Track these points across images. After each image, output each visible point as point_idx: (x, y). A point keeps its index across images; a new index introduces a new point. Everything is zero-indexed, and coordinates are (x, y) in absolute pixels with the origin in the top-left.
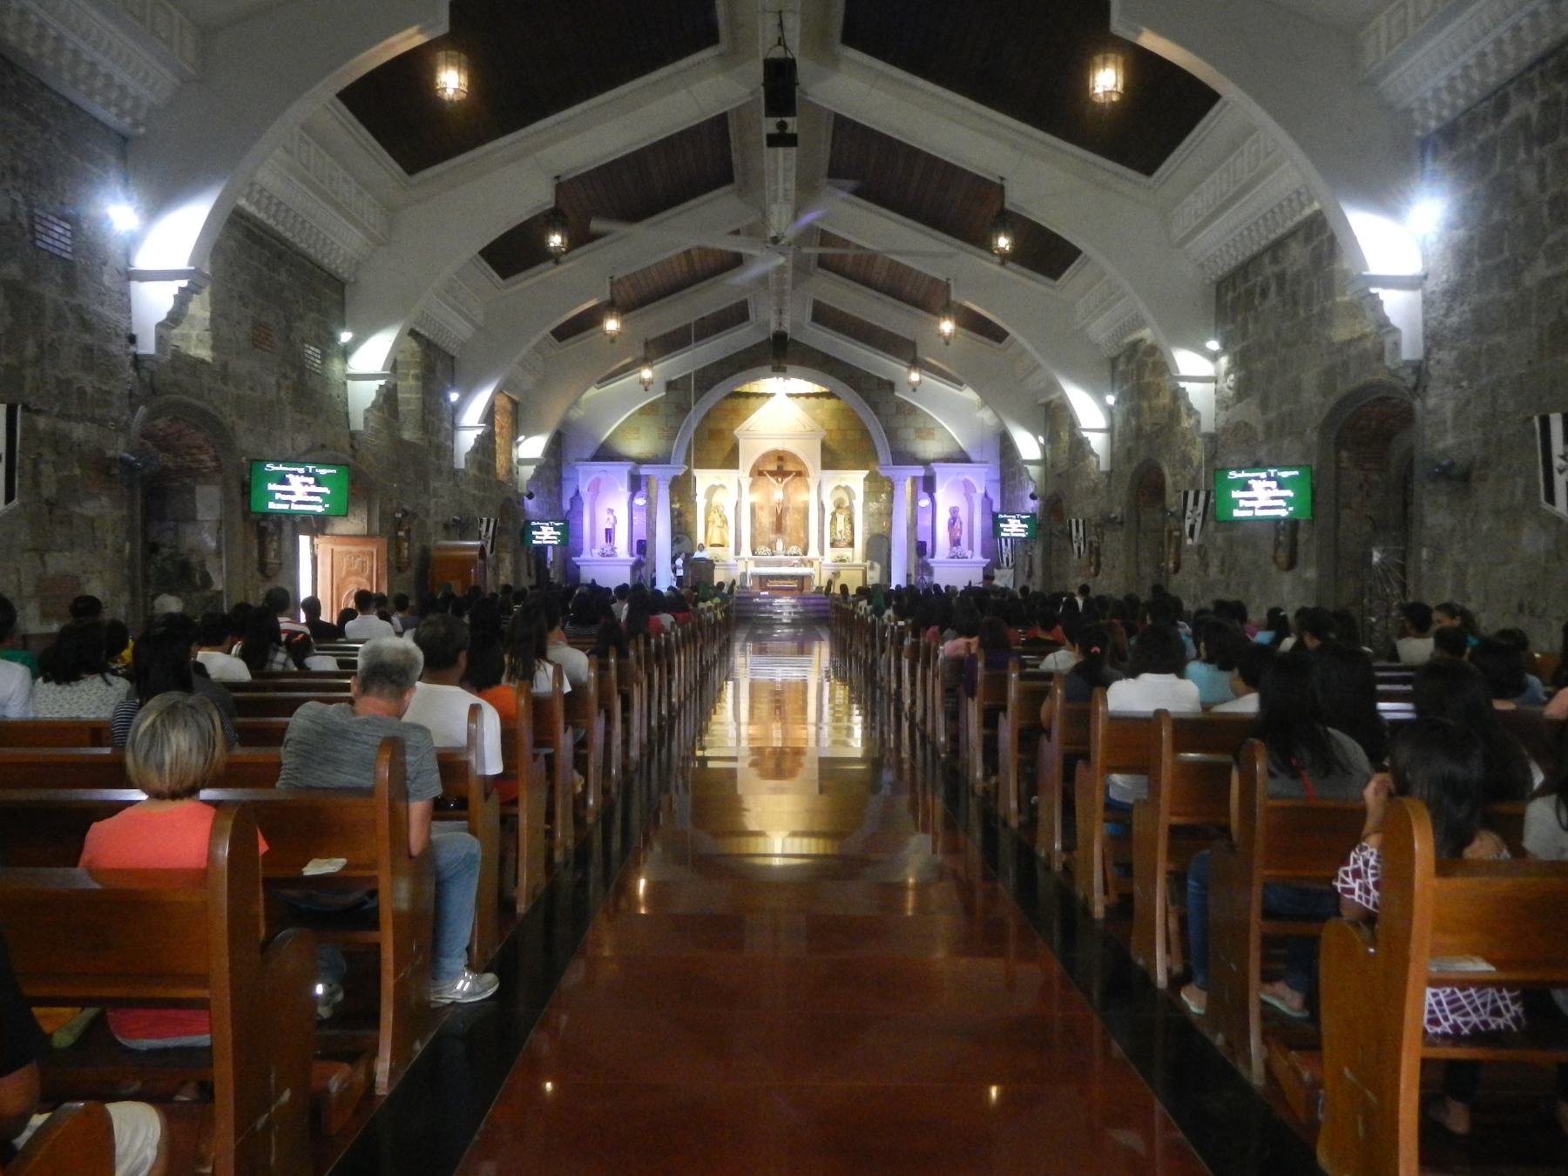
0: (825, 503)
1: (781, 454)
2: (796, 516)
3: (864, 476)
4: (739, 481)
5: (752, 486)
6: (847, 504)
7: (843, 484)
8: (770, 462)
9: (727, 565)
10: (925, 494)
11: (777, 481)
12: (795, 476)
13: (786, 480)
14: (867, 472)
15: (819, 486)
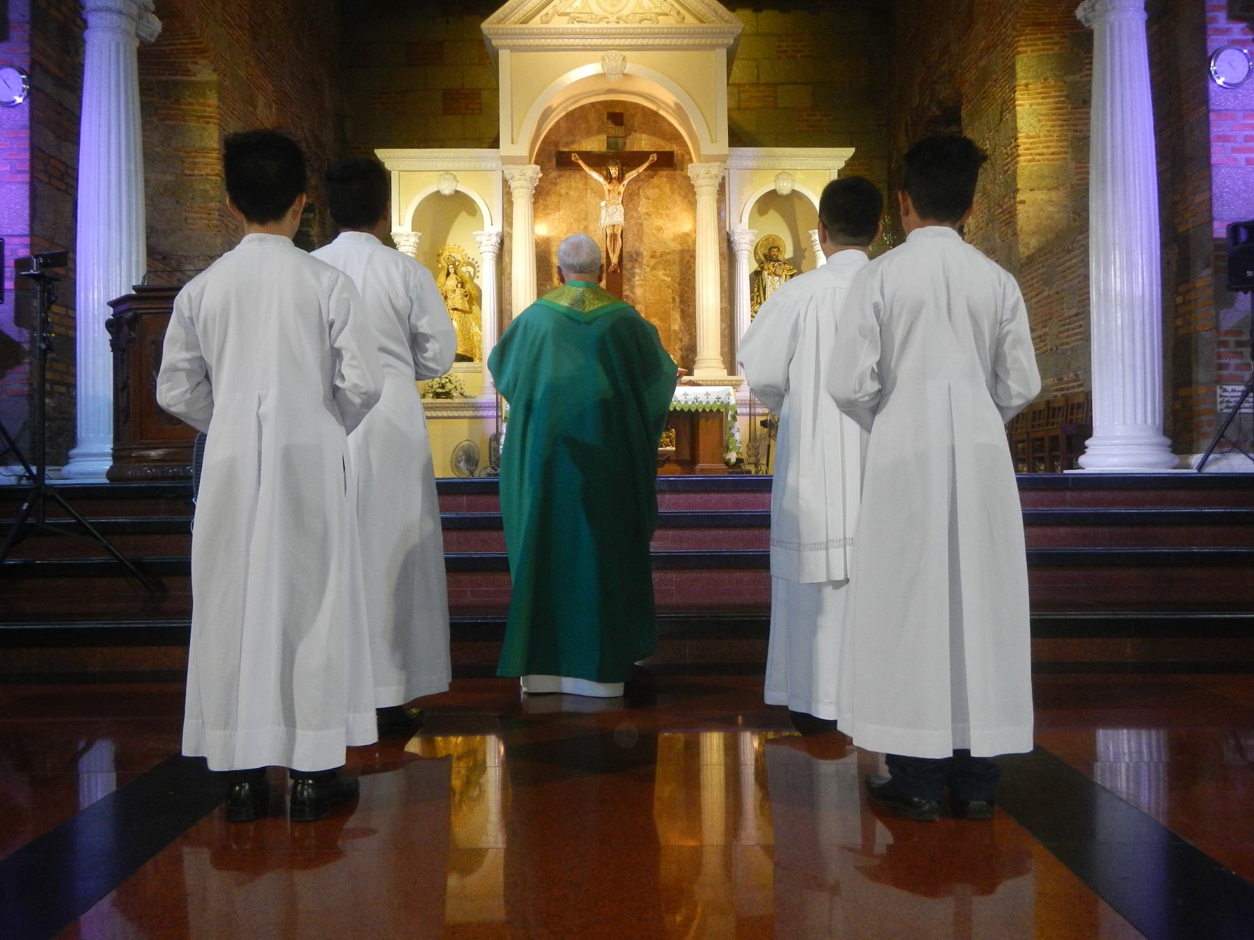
0: (736, 238)
1: (617, 110)
2: (660, 273)
3: (842, 165)
4: (506, 184)
5: (540, 194)
6: (788, 253)
7: (785, 187)
8: (589, 133)
9: (476, 407)
10: (1238, 29)
11: (609, 178)
12: (654, 167)
13: (632, 175)
14: (849, 152)
15: (722, 189)
